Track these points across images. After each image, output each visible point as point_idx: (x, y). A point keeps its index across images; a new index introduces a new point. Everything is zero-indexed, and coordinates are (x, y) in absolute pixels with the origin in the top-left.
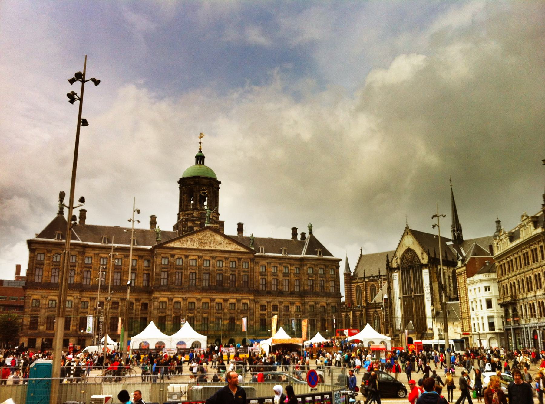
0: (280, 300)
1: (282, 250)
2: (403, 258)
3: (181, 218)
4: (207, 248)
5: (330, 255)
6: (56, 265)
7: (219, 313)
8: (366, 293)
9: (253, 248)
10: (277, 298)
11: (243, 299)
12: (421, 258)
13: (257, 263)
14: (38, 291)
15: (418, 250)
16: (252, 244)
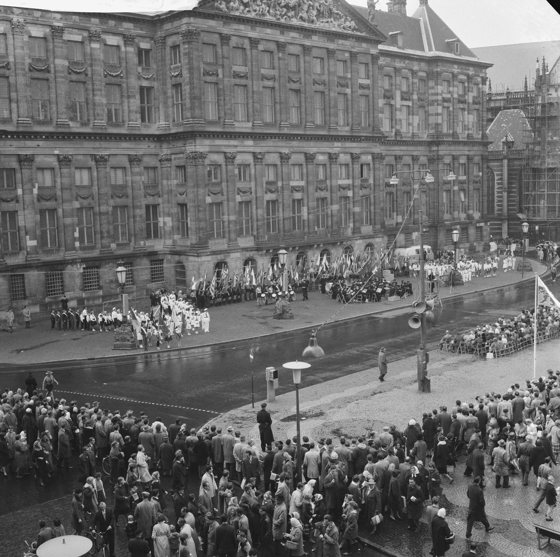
0: (398, 153)
4: (295, 22)
7: (321, 190)
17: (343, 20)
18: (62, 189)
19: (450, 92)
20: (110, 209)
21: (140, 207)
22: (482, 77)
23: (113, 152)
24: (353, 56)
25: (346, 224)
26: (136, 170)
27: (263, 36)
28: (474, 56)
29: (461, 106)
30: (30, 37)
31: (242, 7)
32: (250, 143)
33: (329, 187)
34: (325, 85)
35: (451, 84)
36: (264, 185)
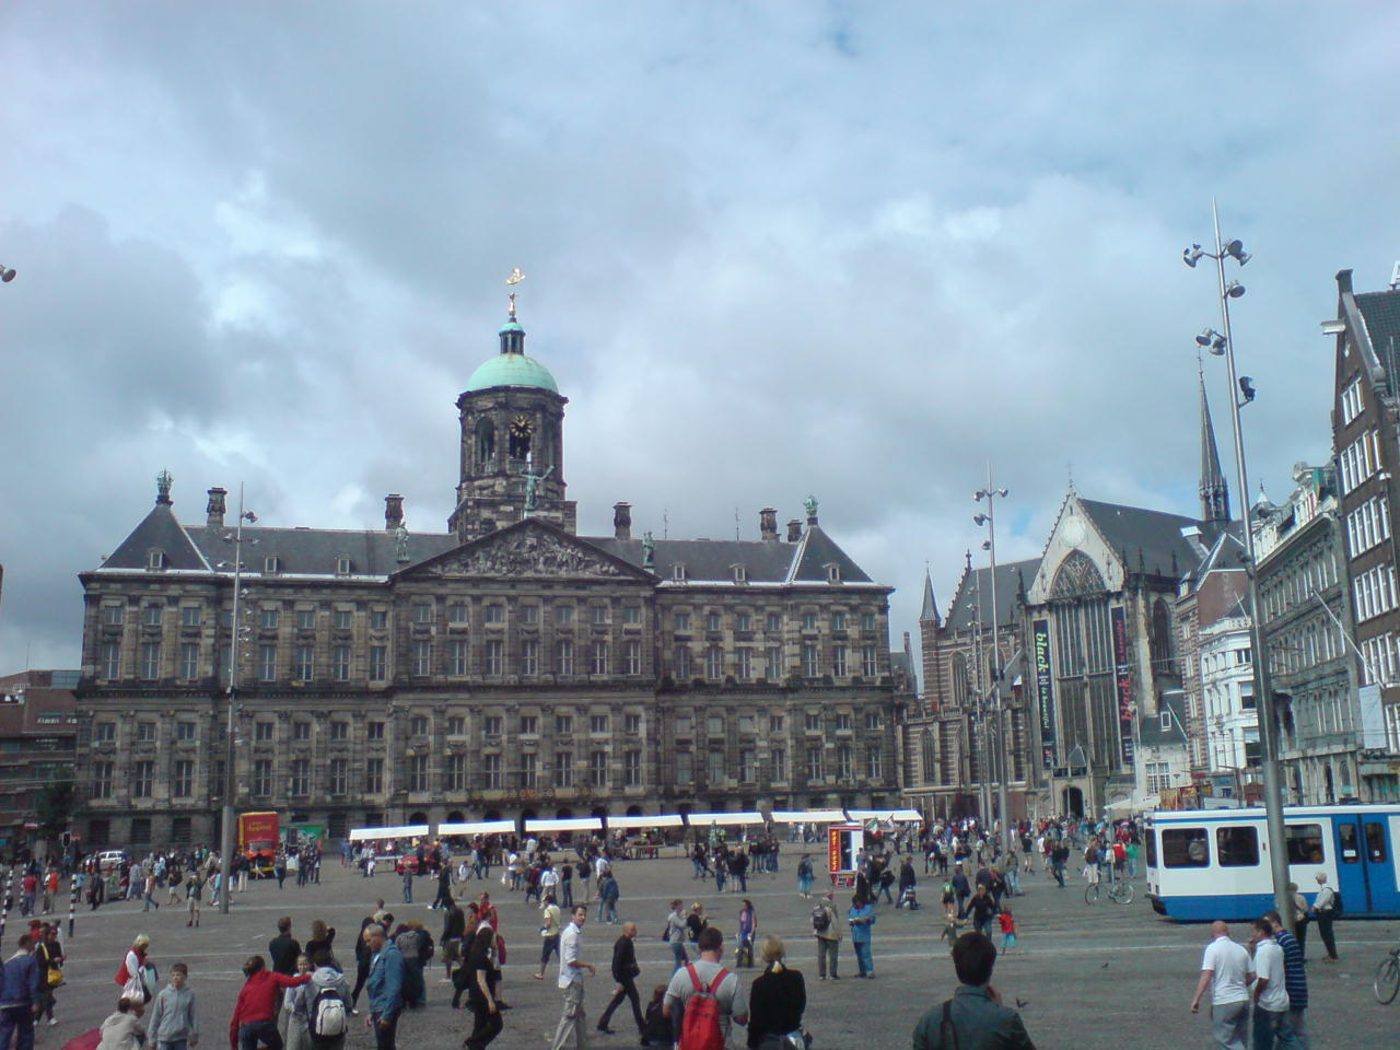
0: (730, 703)
1: (732, 571)
2: (1060, 578)
3: (465, 497)
4: (529, 574)
5: (865, 578)
6: (151, 635)
7: (566, 744)
8: (979, 672)
9: (652, 571)
10: (718, 697)
11: (625, 704)
12: (1105, 578)
13: (666, 608)
14: (110, 701)
15: (1099, 552)
16: (650, 558)
17: (598, 566)
18: (280, 742)
19: (818, 628)
20: (329, 762)
21: (361, 760)
22: (879, 606)
23: (336, 707)
24: (616, 601)
25: (603, 783)
26: (360, 725)
27: (488, 592)
28: (868, 580)
29: (839, 643)
30: (263, 611)
31: (462, 568)
32: (467, 696)
33: (576, 742)
34: (573, 634)
35: (819, 617)
36: (483, 738)
